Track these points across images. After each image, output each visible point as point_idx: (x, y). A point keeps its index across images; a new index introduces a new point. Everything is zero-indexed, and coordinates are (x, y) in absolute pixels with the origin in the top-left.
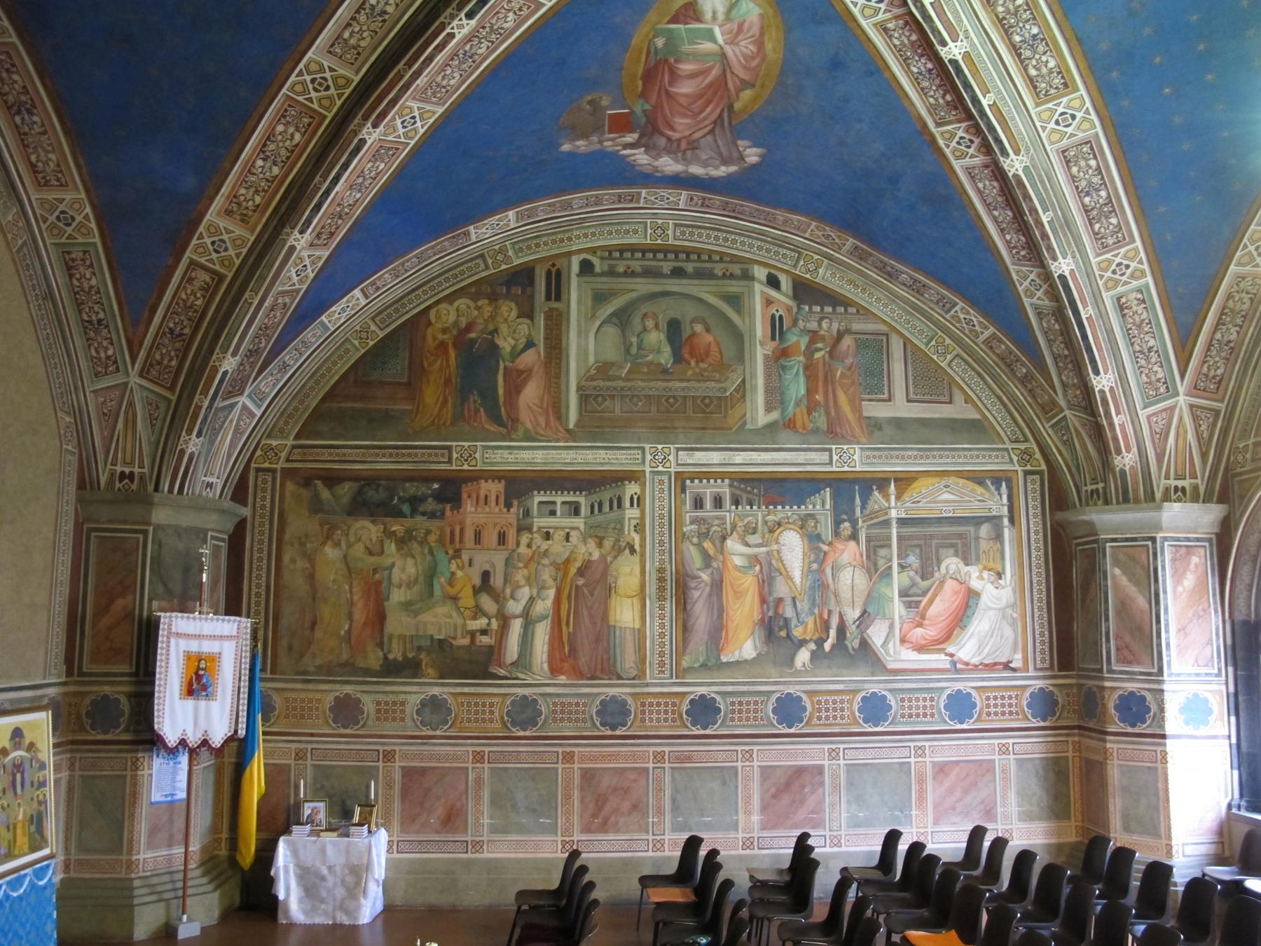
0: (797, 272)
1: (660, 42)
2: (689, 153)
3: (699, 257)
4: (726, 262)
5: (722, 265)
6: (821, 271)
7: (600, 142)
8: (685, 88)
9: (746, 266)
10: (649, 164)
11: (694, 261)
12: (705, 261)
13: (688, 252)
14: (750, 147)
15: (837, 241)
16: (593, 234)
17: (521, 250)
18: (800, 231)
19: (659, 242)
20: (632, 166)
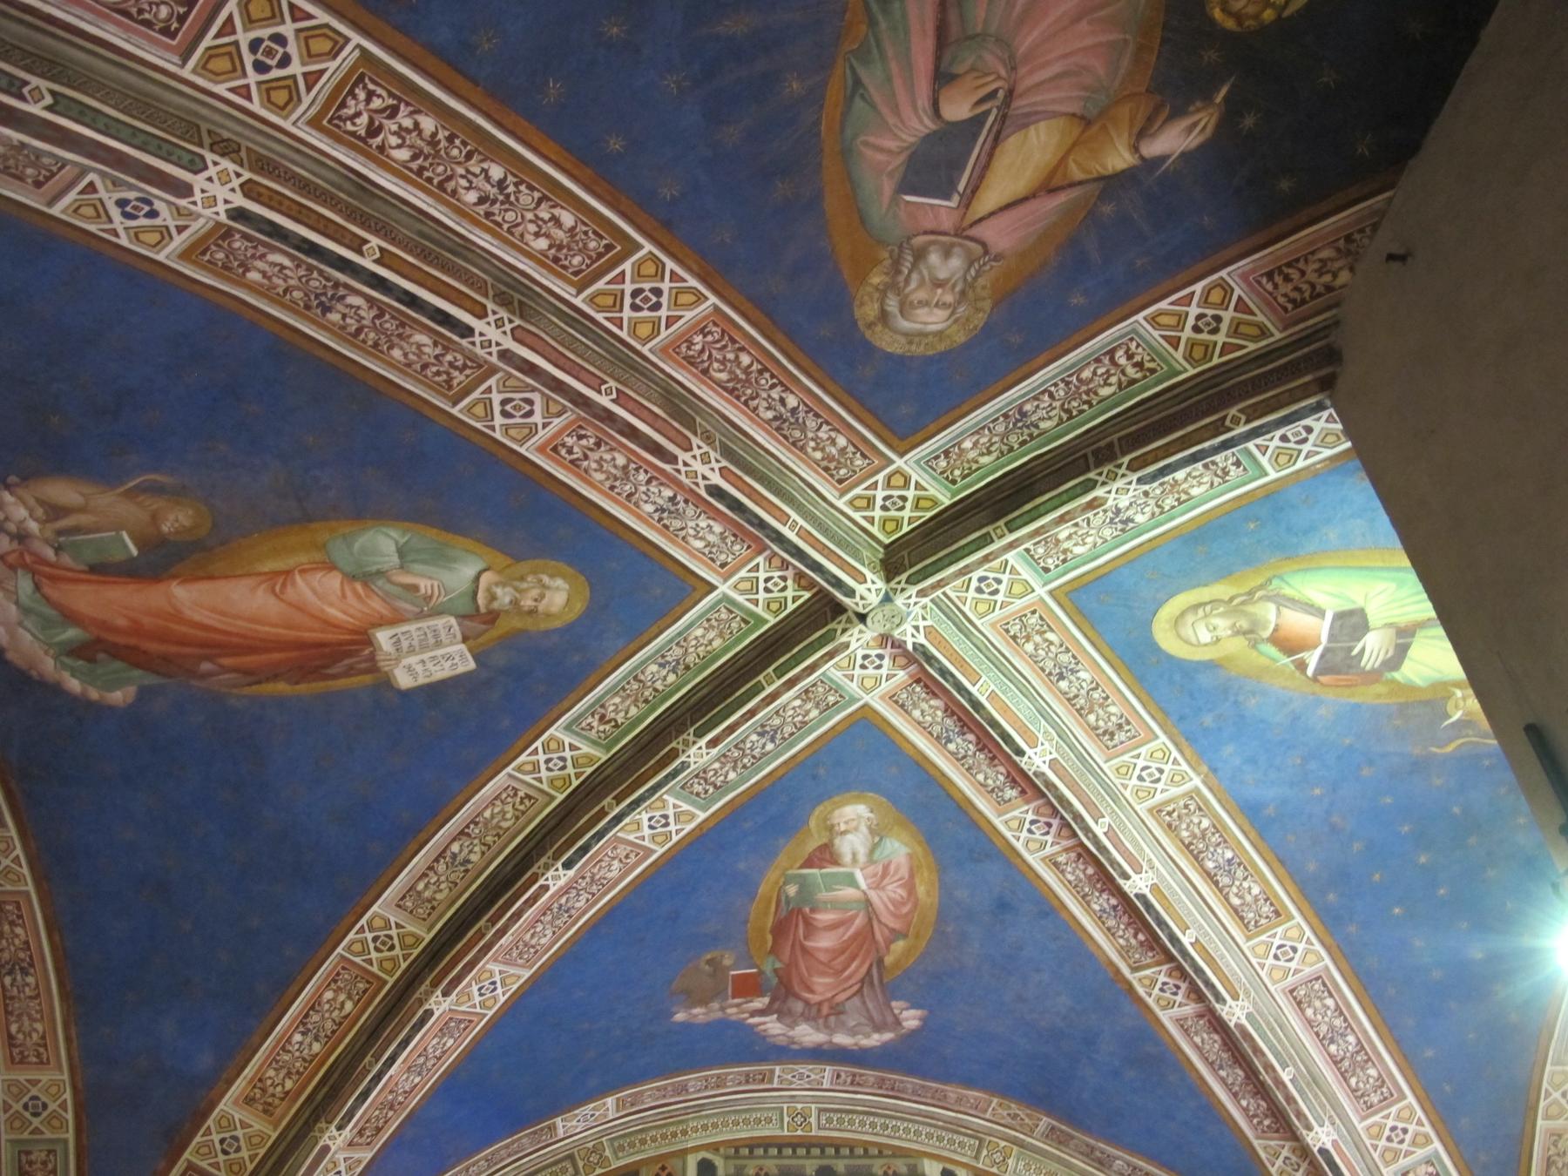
0: (980, 1166)
1: (792, 890)
2: (832, 1019)
3: (852, 1151)
4: (887, 1156)
5: (881, 1161)
6: (1010, 1161)
7: (723, 1009)
8: (824, 942)
9: (911, 1161)
10: (784, 1035)
11: (845, 1157)
12: (860, 1157)
13: (837, 1145)
14: (907, 1009)
15: (1027, 1121)
16: (715, 1126)
17: (622, 1148)
18: (979, 1110)
19: (799, 1133)
20: (763, 1037)
